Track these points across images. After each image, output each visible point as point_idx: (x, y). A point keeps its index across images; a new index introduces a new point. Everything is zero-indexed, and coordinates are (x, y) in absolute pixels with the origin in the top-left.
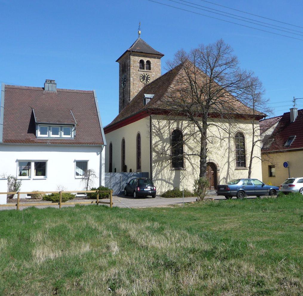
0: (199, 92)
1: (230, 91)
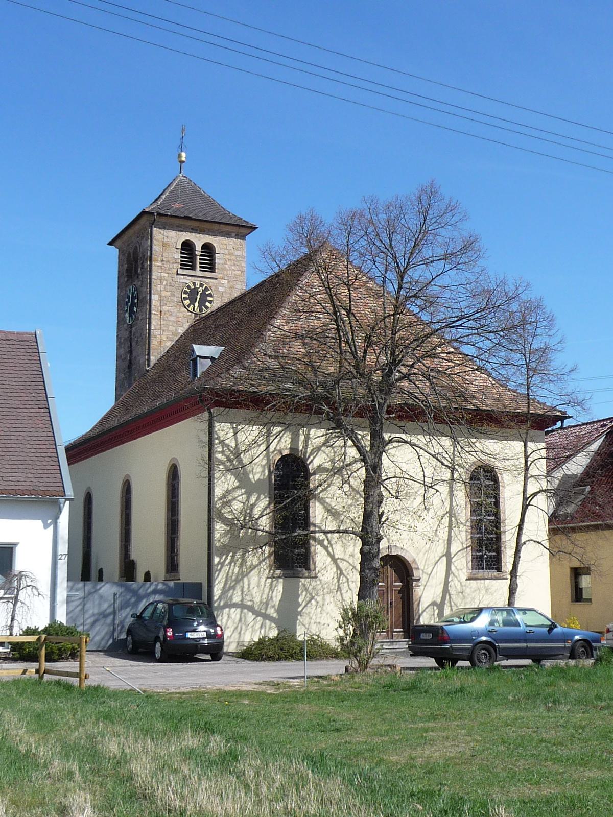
0: (359, 342)
1: (456, 340)
